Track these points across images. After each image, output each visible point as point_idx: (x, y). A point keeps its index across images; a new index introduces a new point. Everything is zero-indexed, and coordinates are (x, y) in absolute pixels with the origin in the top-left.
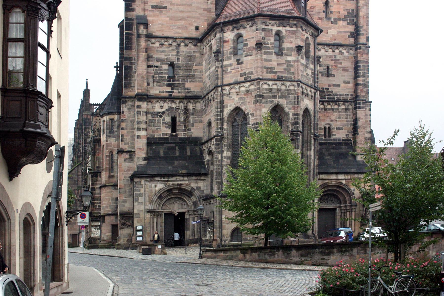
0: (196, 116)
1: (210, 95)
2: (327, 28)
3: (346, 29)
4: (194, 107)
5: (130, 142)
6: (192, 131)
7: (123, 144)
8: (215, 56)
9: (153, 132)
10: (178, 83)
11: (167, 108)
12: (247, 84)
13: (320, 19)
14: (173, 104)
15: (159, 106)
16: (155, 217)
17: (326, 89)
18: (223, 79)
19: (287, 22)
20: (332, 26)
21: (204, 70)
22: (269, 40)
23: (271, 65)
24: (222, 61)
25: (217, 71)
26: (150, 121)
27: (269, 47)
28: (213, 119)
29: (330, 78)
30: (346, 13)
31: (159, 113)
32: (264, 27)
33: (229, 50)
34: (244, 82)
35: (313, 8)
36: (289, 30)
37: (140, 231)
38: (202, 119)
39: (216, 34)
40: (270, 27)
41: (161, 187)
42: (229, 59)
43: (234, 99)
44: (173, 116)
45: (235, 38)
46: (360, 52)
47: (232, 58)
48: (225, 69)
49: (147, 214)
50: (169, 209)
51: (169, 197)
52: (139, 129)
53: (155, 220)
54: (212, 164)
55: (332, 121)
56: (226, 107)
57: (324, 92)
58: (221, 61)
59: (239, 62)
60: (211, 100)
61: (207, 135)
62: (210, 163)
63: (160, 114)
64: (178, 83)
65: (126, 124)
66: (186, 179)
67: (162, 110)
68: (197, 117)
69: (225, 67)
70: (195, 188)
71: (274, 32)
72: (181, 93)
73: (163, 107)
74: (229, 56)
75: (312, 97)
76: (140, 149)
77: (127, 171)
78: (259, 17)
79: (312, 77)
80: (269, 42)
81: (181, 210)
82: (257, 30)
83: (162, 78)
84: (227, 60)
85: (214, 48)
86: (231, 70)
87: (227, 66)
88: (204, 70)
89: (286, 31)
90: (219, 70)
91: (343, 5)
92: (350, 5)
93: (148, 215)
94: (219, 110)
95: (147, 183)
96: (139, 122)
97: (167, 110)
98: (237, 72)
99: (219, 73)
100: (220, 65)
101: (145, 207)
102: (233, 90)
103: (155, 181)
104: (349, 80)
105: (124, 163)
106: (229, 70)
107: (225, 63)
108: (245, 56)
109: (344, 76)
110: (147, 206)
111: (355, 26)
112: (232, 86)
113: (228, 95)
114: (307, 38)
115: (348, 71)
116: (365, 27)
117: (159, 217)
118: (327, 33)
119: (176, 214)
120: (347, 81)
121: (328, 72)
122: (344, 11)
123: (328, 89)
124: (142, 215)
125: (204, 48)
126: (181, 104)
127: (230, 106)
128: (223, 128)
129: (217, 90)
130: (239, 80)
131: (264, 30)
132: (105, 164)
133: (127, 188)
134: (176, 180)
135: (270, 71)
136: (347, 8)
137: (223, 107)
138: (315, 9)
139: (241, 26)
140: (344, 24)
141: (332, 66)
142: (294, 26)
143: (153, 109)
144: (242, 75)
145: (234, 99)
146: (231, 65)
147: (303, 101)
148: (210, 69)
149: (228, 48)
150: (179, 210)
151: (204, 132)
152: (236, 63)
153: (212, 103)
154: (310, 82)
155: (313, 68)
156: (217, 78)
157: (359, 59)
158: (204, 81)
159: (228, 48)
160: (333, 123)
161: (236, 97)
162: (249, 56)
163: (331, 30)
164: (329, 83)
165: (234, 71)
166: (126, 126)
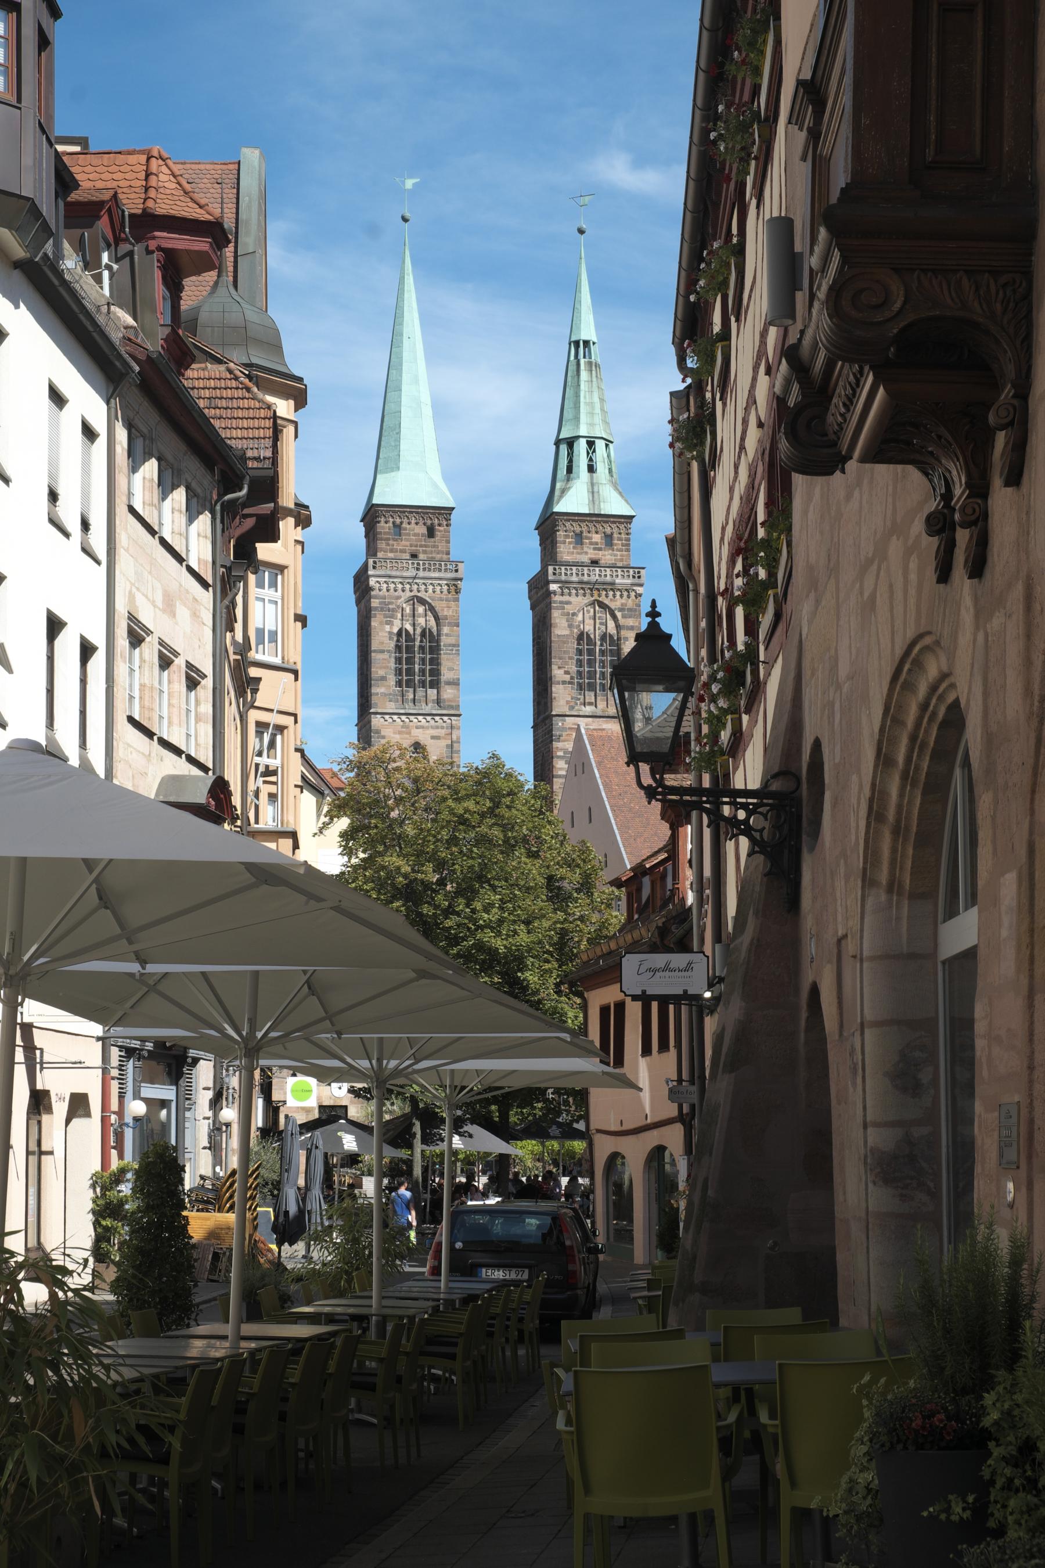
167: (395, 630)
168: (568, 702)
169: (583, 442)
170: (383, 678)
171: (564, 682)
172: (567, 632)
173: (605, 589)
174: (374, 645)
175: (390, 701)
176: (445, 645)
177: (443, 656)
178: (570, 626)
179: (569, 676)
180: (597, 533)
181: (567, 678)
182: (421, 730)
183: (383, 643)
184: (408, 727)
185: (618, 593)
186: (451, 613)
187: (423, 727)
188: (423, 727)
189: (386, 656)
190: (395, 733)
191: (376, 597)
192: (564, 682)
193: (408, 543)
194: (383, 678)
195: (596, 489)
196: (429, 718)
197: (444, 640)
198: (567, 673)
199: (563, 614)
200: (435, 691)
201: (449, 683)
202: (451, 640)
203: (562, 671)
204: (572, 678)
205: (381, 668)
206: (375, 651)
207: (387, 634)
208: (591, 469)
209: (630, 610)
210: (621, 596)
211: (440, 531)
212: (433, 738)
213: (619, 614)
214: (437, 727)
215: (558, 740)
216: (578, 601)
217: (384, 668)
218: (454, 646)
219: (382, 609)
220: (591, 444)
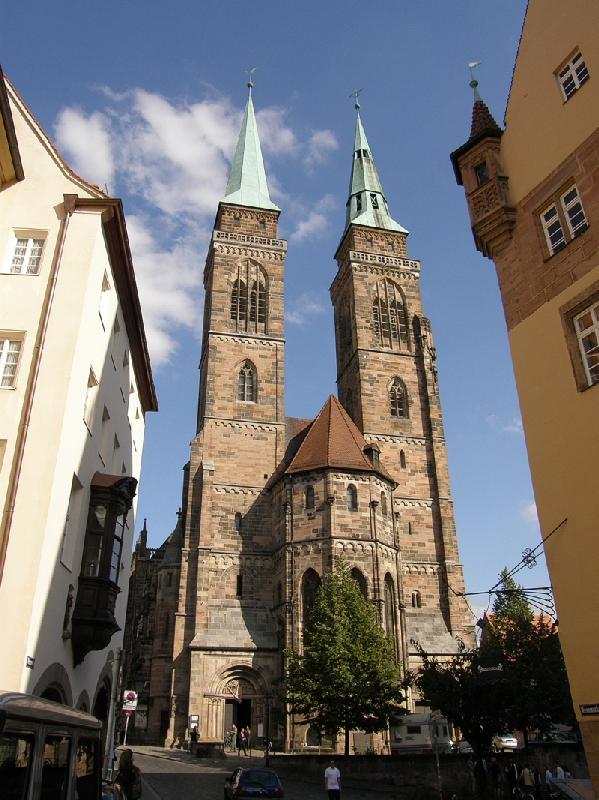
26: (214, 579)
53: (214, 707)
67: (224, 567)
81: (245, 697)
87: (297, 520)
93: (206, 701)
96: (201, 580)
124: (199, 699)
132: (160, 629)
167: (233, 280)
169: (368, 193)
170: (221, 310)
171: (366, 328)
174: (215, 287)
178: (368, 292)
184: (240, 346)
185: (402, 276)
187: (253, 348)
188: (253, 348)
191: (218, 256)
192: (366, 328)
194: (221, 310)
198: (368, 322)
200: (263, 324)
203: (364, 320)
208: (376, 207)
213: (404, 289)
214: (264, 349)
215: (364, 368)
216: (372, 277)
220: (373, 196)
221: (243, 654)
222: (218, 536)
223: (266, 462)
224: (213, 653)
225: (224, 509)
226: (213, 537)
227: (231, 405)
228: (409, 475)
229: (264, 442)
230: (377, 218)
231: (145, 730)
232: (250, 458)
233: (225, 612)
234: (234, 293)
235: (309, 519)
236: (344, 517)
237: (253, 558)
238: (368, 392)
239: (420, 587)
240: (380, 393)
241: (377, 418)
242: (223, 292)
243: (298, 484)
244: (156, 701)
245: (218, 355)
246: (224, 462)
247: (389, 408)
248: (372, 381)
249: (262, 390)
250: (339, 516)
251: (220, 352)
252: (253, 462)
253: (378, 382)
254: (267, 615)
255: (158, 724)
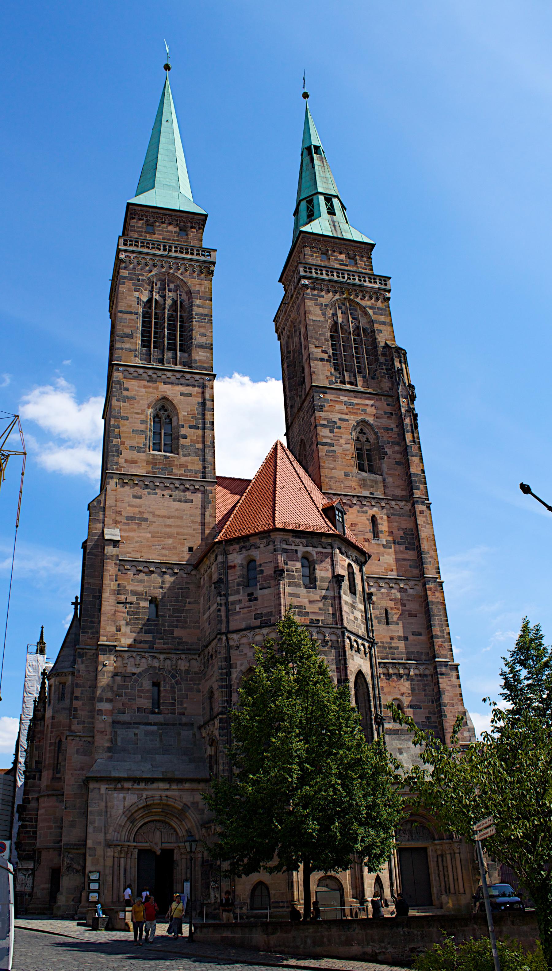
0: (190, 681)
1: (210, 648)
2: (378, 553)
3: (407, 557)
4: (187, 668)
5: (86, 721)
6: (185, 706)
7: (76, 723)
8: (215, 588)
9: (123, 706)
10: (163, 629)
11: (146, 666)
12: (265, 631)
13: (366, 540)
14: (155, 660)
15: (133, 663)
16: (123, 855)
17: (387, 643)
18: (228, 622)
19: (319, 540)
20: (385, 552)
21: (202, 611)
22: (294, 566)
23: (300, 602)
24: (226, 595)
25: (219, 610)
27: (294, 575)
28: (215, 686)
29: (391, 627)
30: (401, 533)
31: (134, 674)
32: (285, 546)
33: (236, 579)
34: (260, 627)
35: (355, 526)
36: (321, 553)
37: (94, 881)
38: (200, 687)
39: (216, 556)
40: (293, 547)
41: (134, 801)
42: (238, 592)
43: (246, 654)
44: (155, 680)
45: (245, 563)
46: (430, 588)
47: (241, 590)
48: (230, 607)
49: (109, 850)
50: (146, 842)
51: (146, 820)
52: (101, 700)
54: (217, 763)
55: (402, 694)
56: (234, 666)
57: (385, 648)
58: (224, 595)
59: (252, 598)
60: (212, 656)
61: (208, 713)
62: (213, 760)
63: (136, 676)
64: (163, 629)
65: (82, 690)
66: (174, 787)
68: (191, 683)
69: (232, 604)
70: (189, 804)
71: (300, 555)
72: (168, 644)
73: (139, 664)
74: (236, 588)
75: (366, 654)
76: (102, 732)
77: (79, 770)
78: (278, 533)
79: (363, 623)
80: (294, 569)
81: (166, 846)
82: (275, 550)
83: (139, 620)
84: (235, 595)
85: (215, 577)
86: (240, 609)
87: (234, 603)
88: (202, 611)
89: (317, 553)
90: (223, 608)
91: (397, 522)
92: (405, 522)
94: (224, 671)
95: (110, 792)
97: (145, 671)
98: (249, 612)
99: (223, 613)
100: (223, 602)
101: (105, 837)
102: (244, 641)
103: (123, 789)
104: (420, 630)
105: (76, 756)
106: (238, 610)
107: (231, 599)
108: (260, 589)
109: (412, 623)
110: (108, 835)
111: (418, 552)
112: (242, 633)
113: (238, 647)
114: (349, 565)
115: (416, 617)
116: (432, 553)
117: (129, 855)
118: (379, 561)
119: (159, 852)
120: (418, 632)
121: (387, 618)
122: (398, 530)
123: (391, 643)
125: (201, 578)
126: (168, 662)
127: (241, 665)
128: (231, 700)
129: (220, 639)
130: (252, 625)
131: (285, 551)
133: (78, 800)
134: (158, 789)
135: (298, 612)
136: (403, 527)
137: (230, 666)
138: (357, 527)
139: (251, 546)
140: (401, 549)
141: (392, 609)
142: (329, 547)
143: (125, 668)
144: (256, 617)
145: (246, 654)
146: (240, 601)
147: (353, 659)
148: (209, 609)
149: (234, 576)
150: (163, 845)
151: (204, 709)
152: (247, 598)
153: (214, 661)
154: (362, 631)
155: (363, 609)
156: (220, 622)
157: (430, 599)
158: (201, 628)
159: (234, 576)
160: (404, 697)
161: (250, 652)
162: (265, 588)
163: (383, 556)
164: (391, 635)
165: (245, 610)
166: (82, 693)
167: (145, 299)
168: (327, 377)
170: (130, 336)
171: (322, 360)
172: (322, 319)
173: (355, 290)
175: (136, 356)
176: (196, 314)
177: (194, 323)
179: (327, 355)
180: (341, 253)
181: (325, 356)
182: (169, 386)
183: (130, 306)
186: (203, 289)
187: (172, 384)
189: (134, 317)
190: (138, 387)
192: (322, 360)
193: (161, 237)
194: (130, 336)
195: (337, 224)
196: (178, 375)
197: (196, 310)
198: (324, 352)
199: (316, 305)
201: (201, 346)
202: (201, 311)
203: (319, 350)
204: (329, 357)
205: (128, 327)
206: (121, 312)
207: (136, 299)
209: (379, 309)
210: (371, 298)
211: (192, 232)
212: (182, 394)
213: (370, 312)
214: (188, 385)
217: (131, 327)
218: (206, 315)
219: (131, 279)
221: (161, 785)
222: (126, 629)
223: (191, 531)
224: (119, 786)
225: (134, 593)
226: (119, 630)
227: (143, 456)
228: (384, 546)
229: (189, 505)
230: (334, 225)
231: (31, 895)
232: (169, 526)
233: (136, 731)
234: (146, 316)
235: (250, 600)
236: (298, 596)
237: (174, 657)
238: (329, 441)
239: (402, 694)
240: (342, 441)
241: (339, 474)
242: (131, 313)
243: (235, 555)
244: (44, 854)
245: (125, 393)
246: (134, 531)
247: (354, 462)
248: (332, 425)
249: (185, 437)
250: (291, 595)
251: (127, 390)
252: (174, 530)
253: (339, 428)
254: (194, 735)
255: (48, 886)
